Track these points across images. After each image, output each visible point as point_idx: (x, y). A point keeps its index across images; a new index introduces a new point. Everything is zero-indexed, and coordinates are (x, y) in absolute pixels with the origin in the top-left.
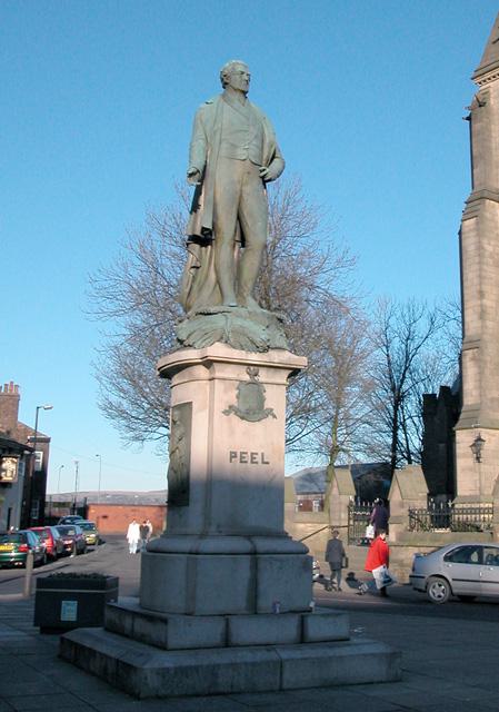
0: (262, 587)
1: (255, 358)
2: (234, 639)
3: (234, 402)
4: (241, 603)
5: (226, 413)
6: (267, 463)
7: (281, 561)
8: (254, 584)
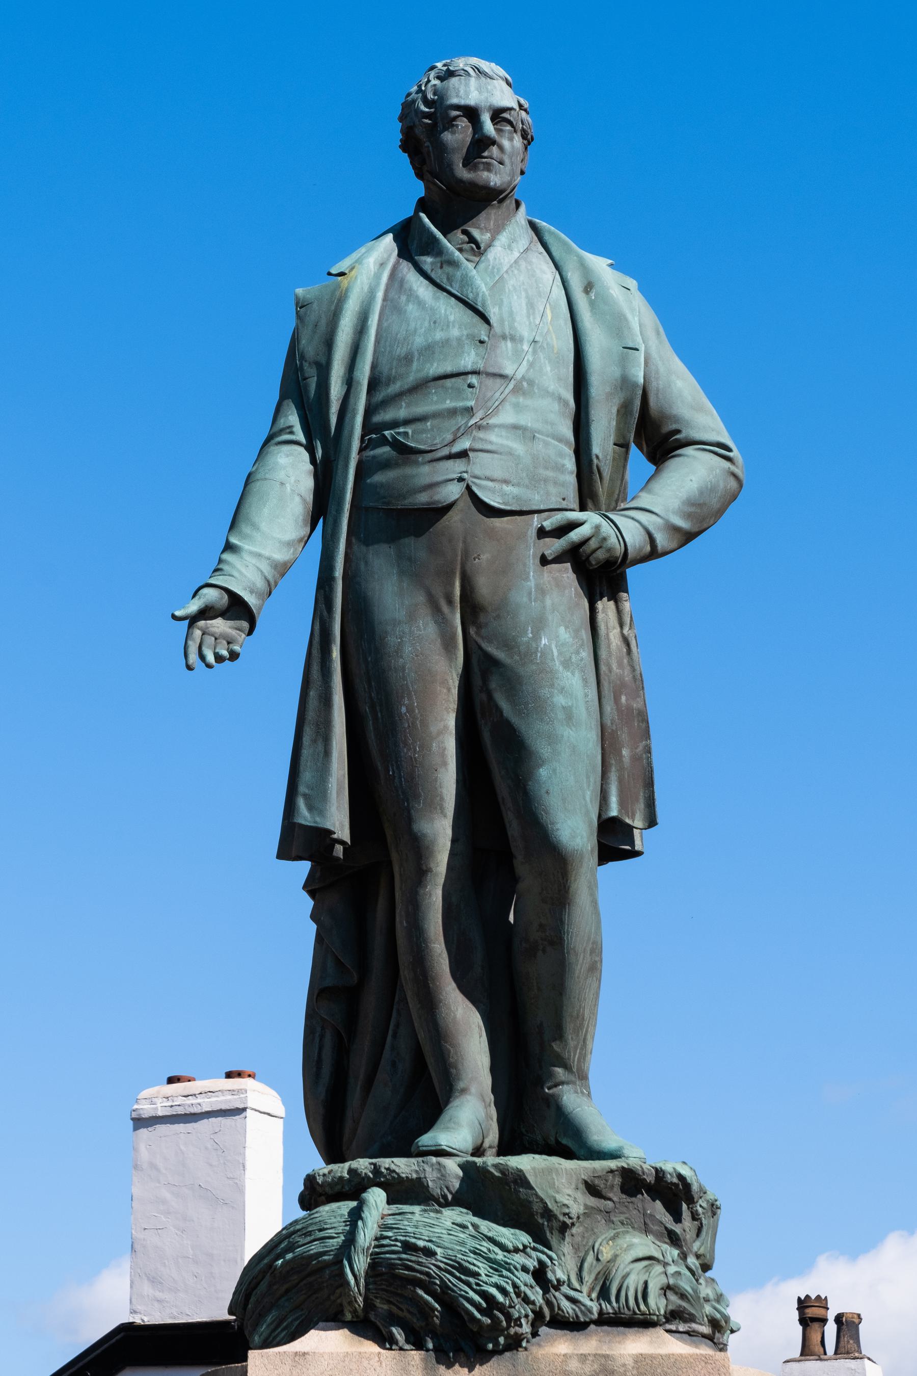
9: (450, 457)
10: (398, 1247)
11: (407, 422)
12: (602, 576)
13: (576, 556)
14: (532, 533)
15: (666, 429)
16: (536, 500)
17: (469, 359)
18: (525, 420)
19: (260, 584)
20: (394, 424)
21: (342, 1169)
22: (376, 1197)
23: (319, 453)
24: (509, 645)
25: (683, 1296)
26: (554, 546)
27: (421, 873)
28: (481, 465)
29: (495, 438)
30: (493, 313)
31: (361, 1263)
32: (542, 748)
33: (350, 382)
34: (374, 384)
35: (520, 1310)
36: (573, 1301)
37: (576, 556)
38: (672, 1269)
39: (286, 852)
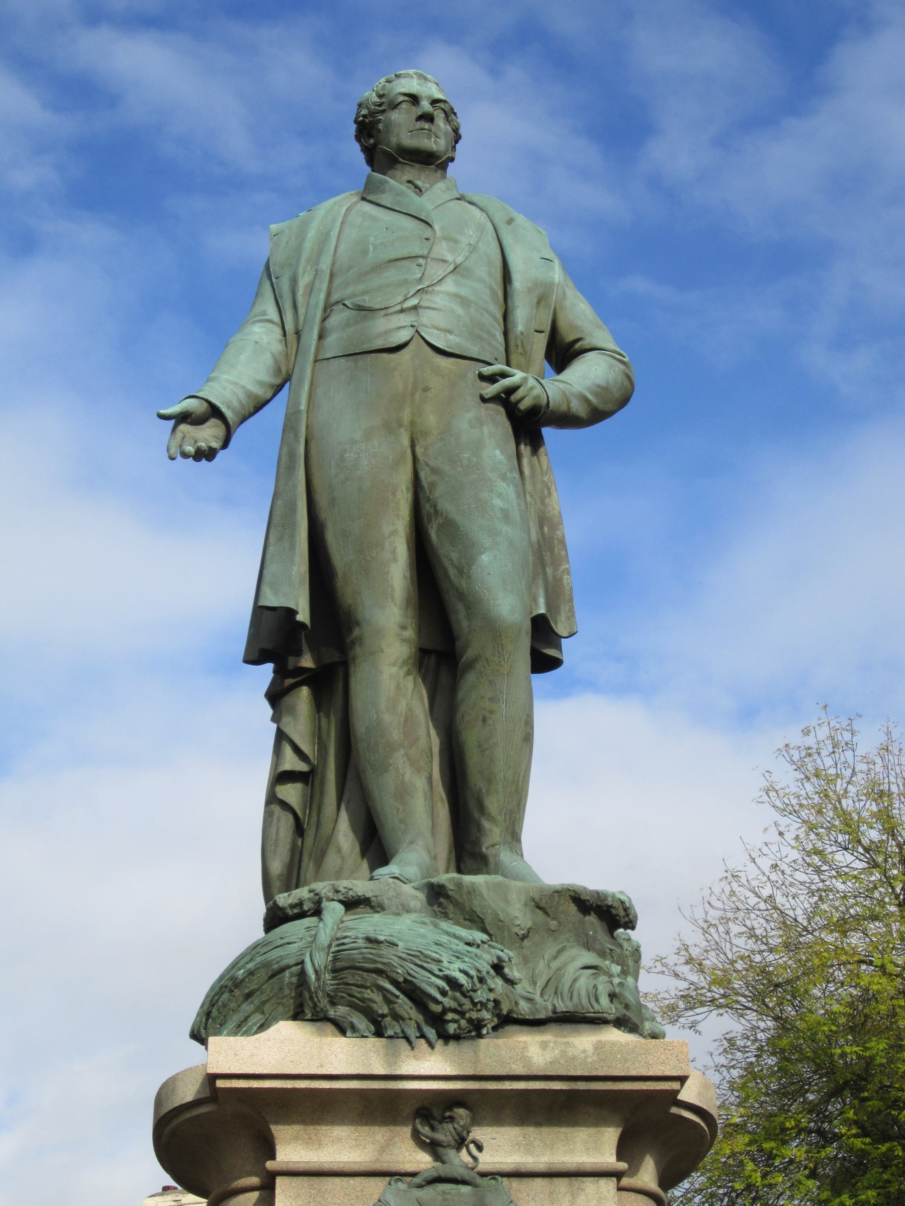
1: (430, 1066)
9: (402, 311)
10: (361, 943)
11: (364, 293)
12: (528, 425)
13: (505, 399)
14: (472, 376)
15: (570, 338)
16: (474, 351)
20: (355, 296)
21: (302, 893)
22: (334, 910)
25: (627, 1007)
26: (491, 390)
28: (427, 318)
36: (530, 1000)
37: (505, 399)
38: (616, 981)
39: (255, 657)
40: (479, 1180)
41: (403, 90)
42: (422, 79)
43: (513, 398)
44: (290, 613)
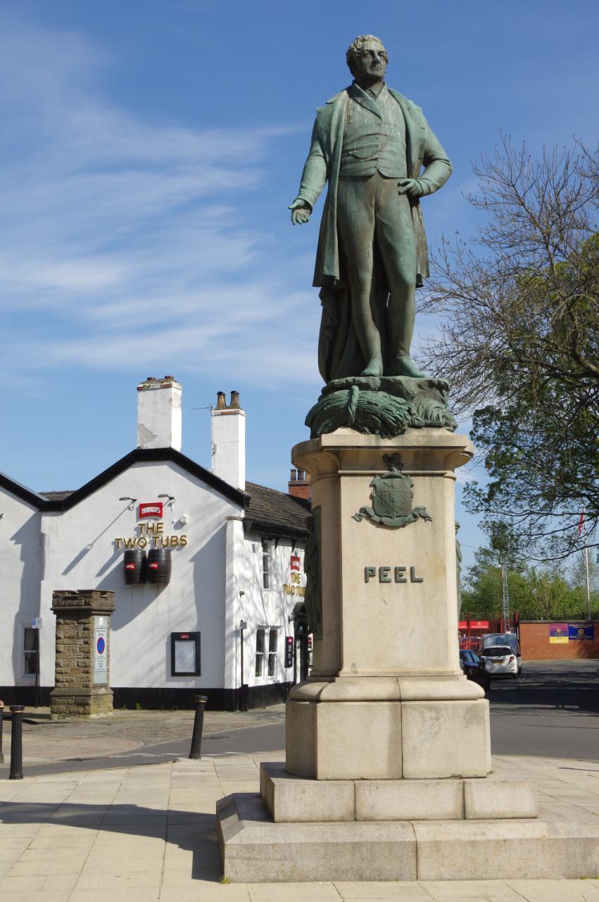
0: (408, 746)
2: (364, 811)
3: (369, 504)
4: (379, 763)
5: (358, 518)
6: (420, 581)
7: (436, 709)
8: (398, 742)
9: (372, 160)
11: (357, 149)
12: (414, 199)
15: (430, 155)
17: (375, 129)
18: (394, 149)
19: (313, 199)
20: (353, 150)
22: (356, 388)
23: (328, 159)
24: (390, 219)
25: (447, 419)
26: (403, 189)
27: (360, 289)
28: (381, 163)
29: (385, 155)
30: (382, 116)
31: (354, 408)
32: (401, 251)
33: (337, 136)
34: (345, 137)
35: (405, 422)
39: (315, 284)
40: (403, 476)
41: (369, 49)
42: (374, 45)
43: (411, 191)
44: (333, 277)
